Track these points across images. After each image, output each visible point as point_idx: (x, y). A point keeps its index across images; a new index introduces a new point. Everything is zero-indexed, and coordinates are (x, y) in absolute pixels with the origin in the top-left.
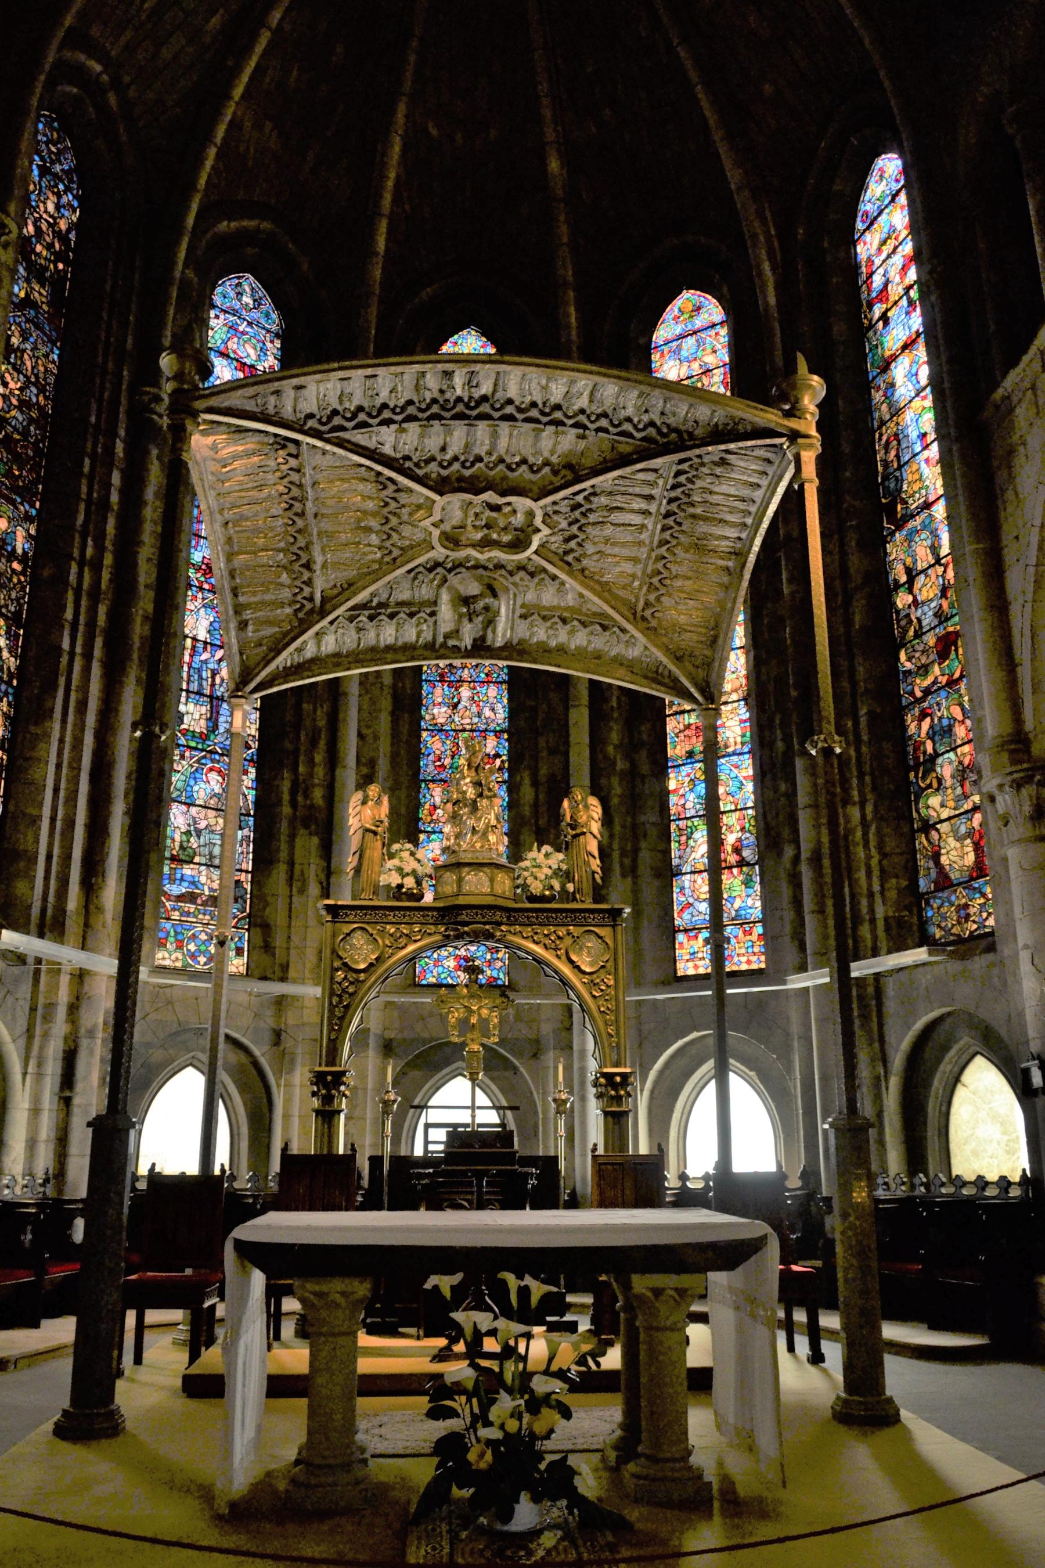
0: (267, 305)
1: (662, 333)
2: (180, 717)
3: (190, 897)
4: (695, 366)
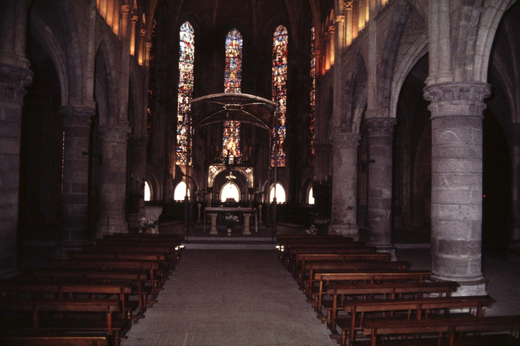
0: (191, 27)
1: (276, 34)
2: (178, 118)
3: (181, 152)
4: (281, 43)
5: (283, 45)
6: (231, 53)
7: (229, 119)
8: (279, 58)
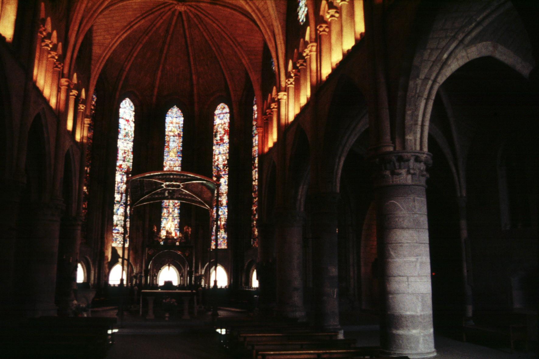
1: (217, 112)
2: (114, 198)
3: (118, 233)
5: (225, 123)
6: (171, 131)
7: (167, 198)
8: (220, 137)
